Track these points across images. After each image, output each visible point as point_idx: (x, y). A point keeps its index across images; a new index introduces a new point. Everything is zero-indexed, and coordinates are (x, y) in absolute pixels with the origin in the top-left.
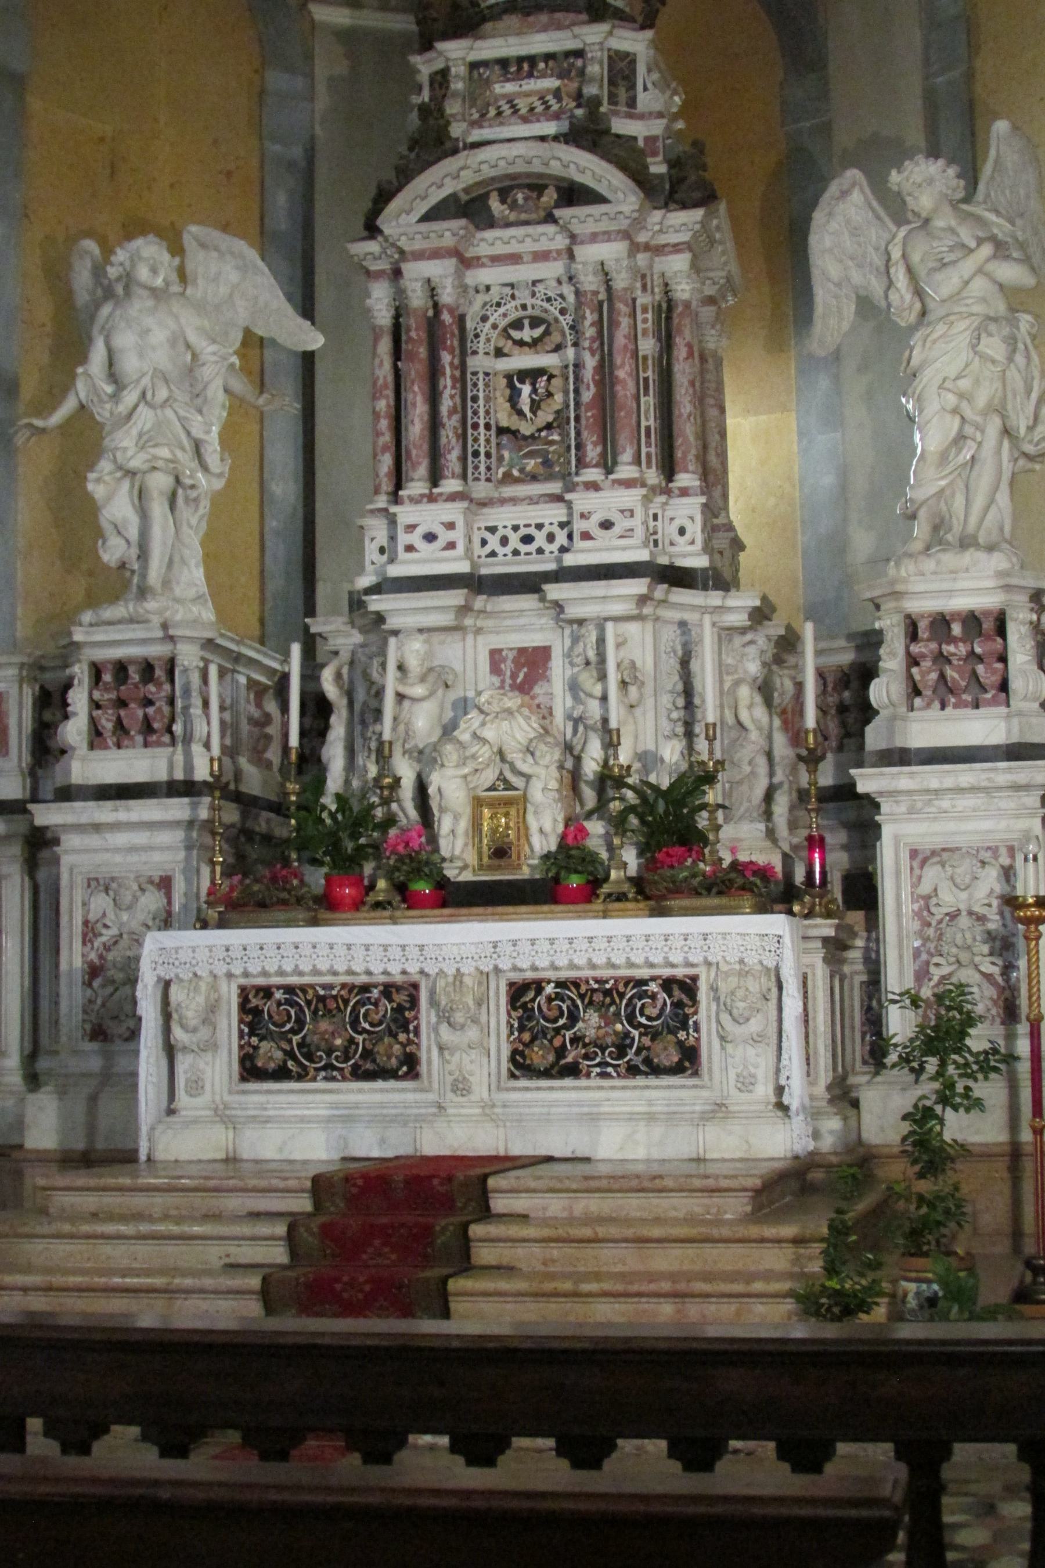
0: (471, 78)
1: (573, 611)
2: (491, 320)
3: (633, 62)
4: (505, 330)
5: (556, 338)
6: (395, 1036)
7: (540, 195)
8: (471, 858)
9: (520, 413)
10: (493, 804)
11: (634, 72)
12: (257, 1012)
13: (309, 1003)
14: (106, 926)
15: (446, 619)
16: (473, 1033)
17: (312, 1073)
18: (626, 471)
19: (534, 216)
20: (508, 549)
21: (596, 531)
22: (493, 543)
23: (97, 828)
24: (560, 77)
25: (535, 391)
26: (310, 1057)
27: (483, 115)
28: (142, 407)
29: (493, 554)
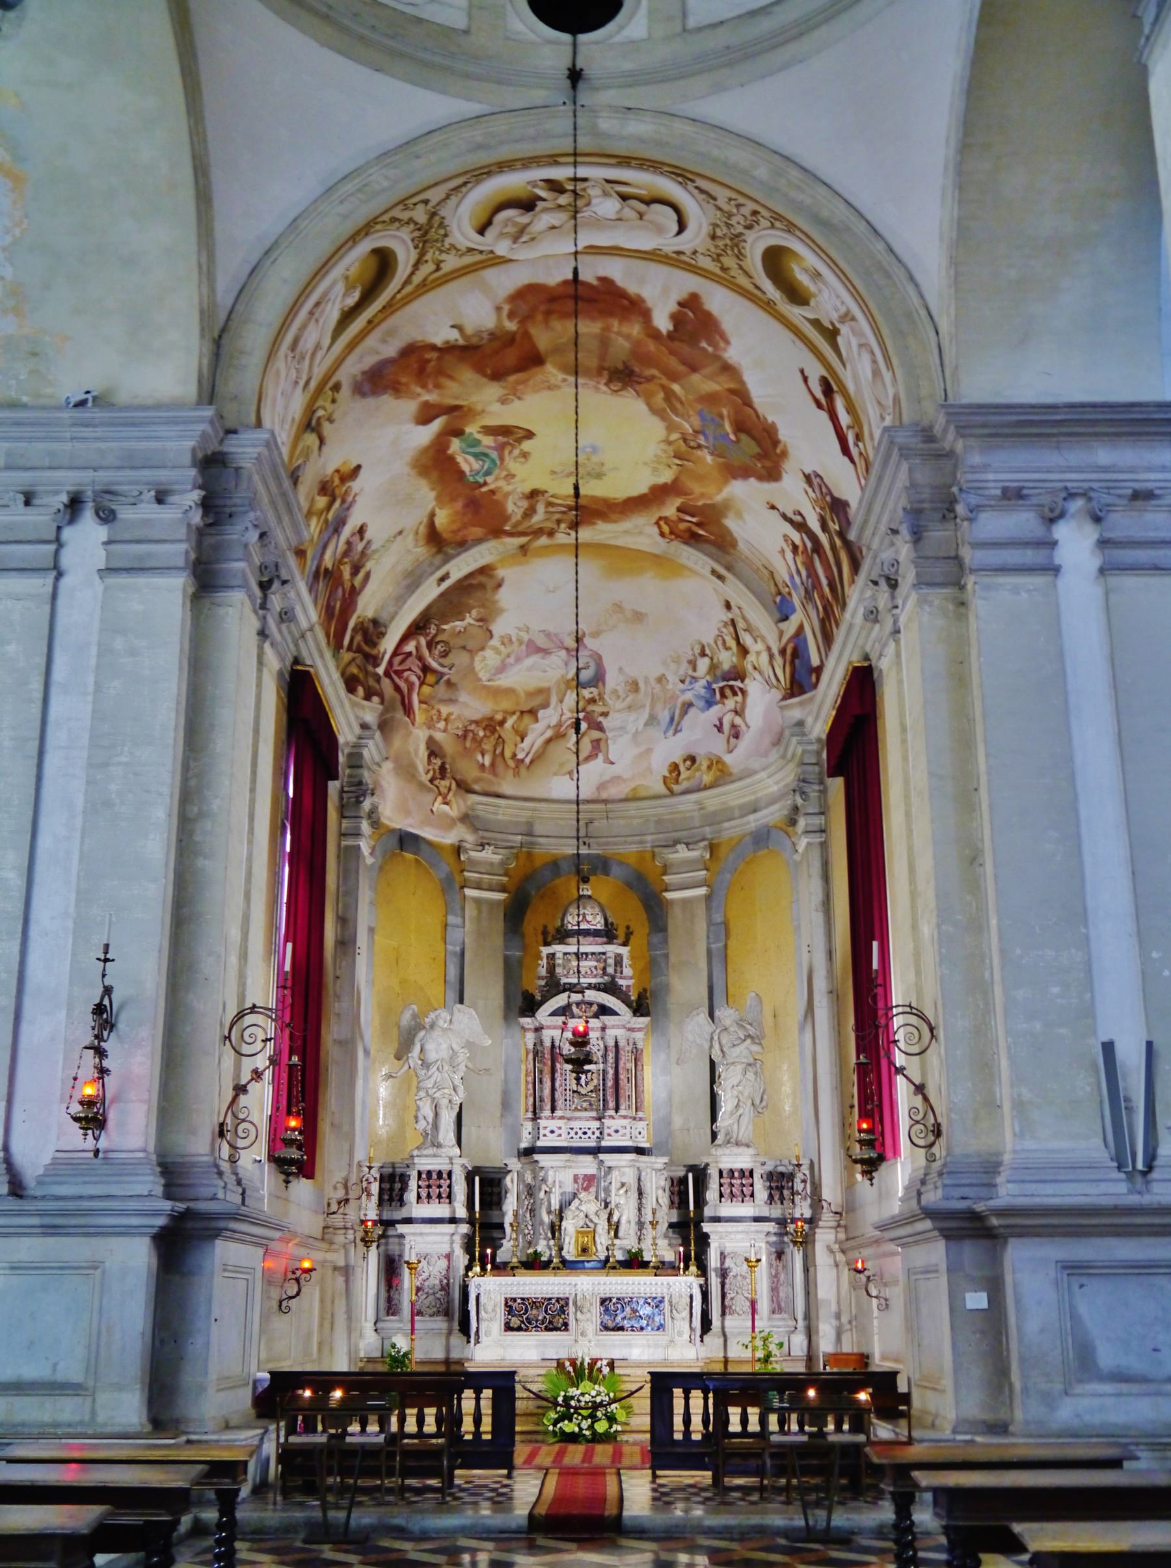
1: (608, 1164)
10: (581, 1232)
12: (511, 1307)
16: (588, 1315)
18: (622, 1112)
21: (613, 1133)
22: (572, 1133)
23: (421, 1234)
26: (530, 1323)
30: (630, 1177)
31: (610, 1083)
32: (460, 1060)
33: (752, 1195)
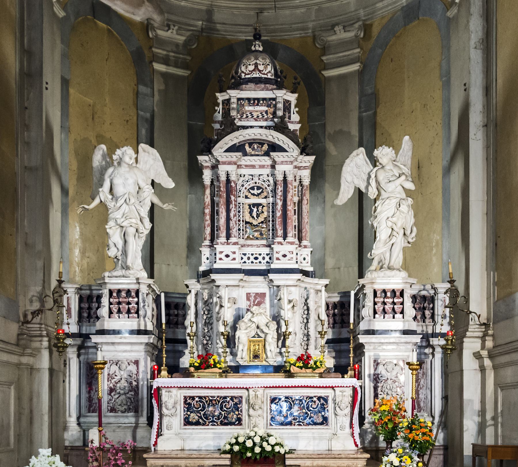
0: (238, 104)
1: (276, 283)
2: (245, 186)
3: (290, 104)
4: (248, 190)
5: (265, 194)
6: (234, 412)
7: (262, 147)
8: (247, 358)
9: (253, 217)
10: (254, 342)
11: (290, 107)
13: (207, 402)
14: (116, 376)
15: (236, 283)
16: (260, 412)
17: (207, 423)
18: (290, 239)
19: (260, 153)
20: (250, 261)
21: (281, 258)
22: (245, 258)
23: (113, 344)
24: (267, 106)
25: (258, 211)
26: (207, 418)
27: (242, 117)
28: (125, 205)
29: (245, 262)
30: (296, 294)
31: (279, 214)
32: (145, 194)
33: (402, 312)
